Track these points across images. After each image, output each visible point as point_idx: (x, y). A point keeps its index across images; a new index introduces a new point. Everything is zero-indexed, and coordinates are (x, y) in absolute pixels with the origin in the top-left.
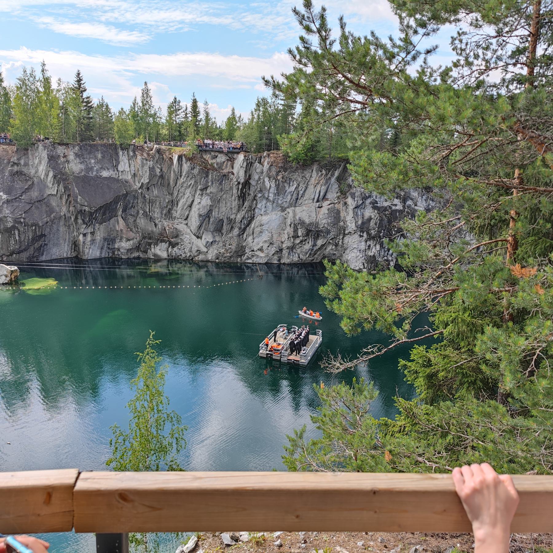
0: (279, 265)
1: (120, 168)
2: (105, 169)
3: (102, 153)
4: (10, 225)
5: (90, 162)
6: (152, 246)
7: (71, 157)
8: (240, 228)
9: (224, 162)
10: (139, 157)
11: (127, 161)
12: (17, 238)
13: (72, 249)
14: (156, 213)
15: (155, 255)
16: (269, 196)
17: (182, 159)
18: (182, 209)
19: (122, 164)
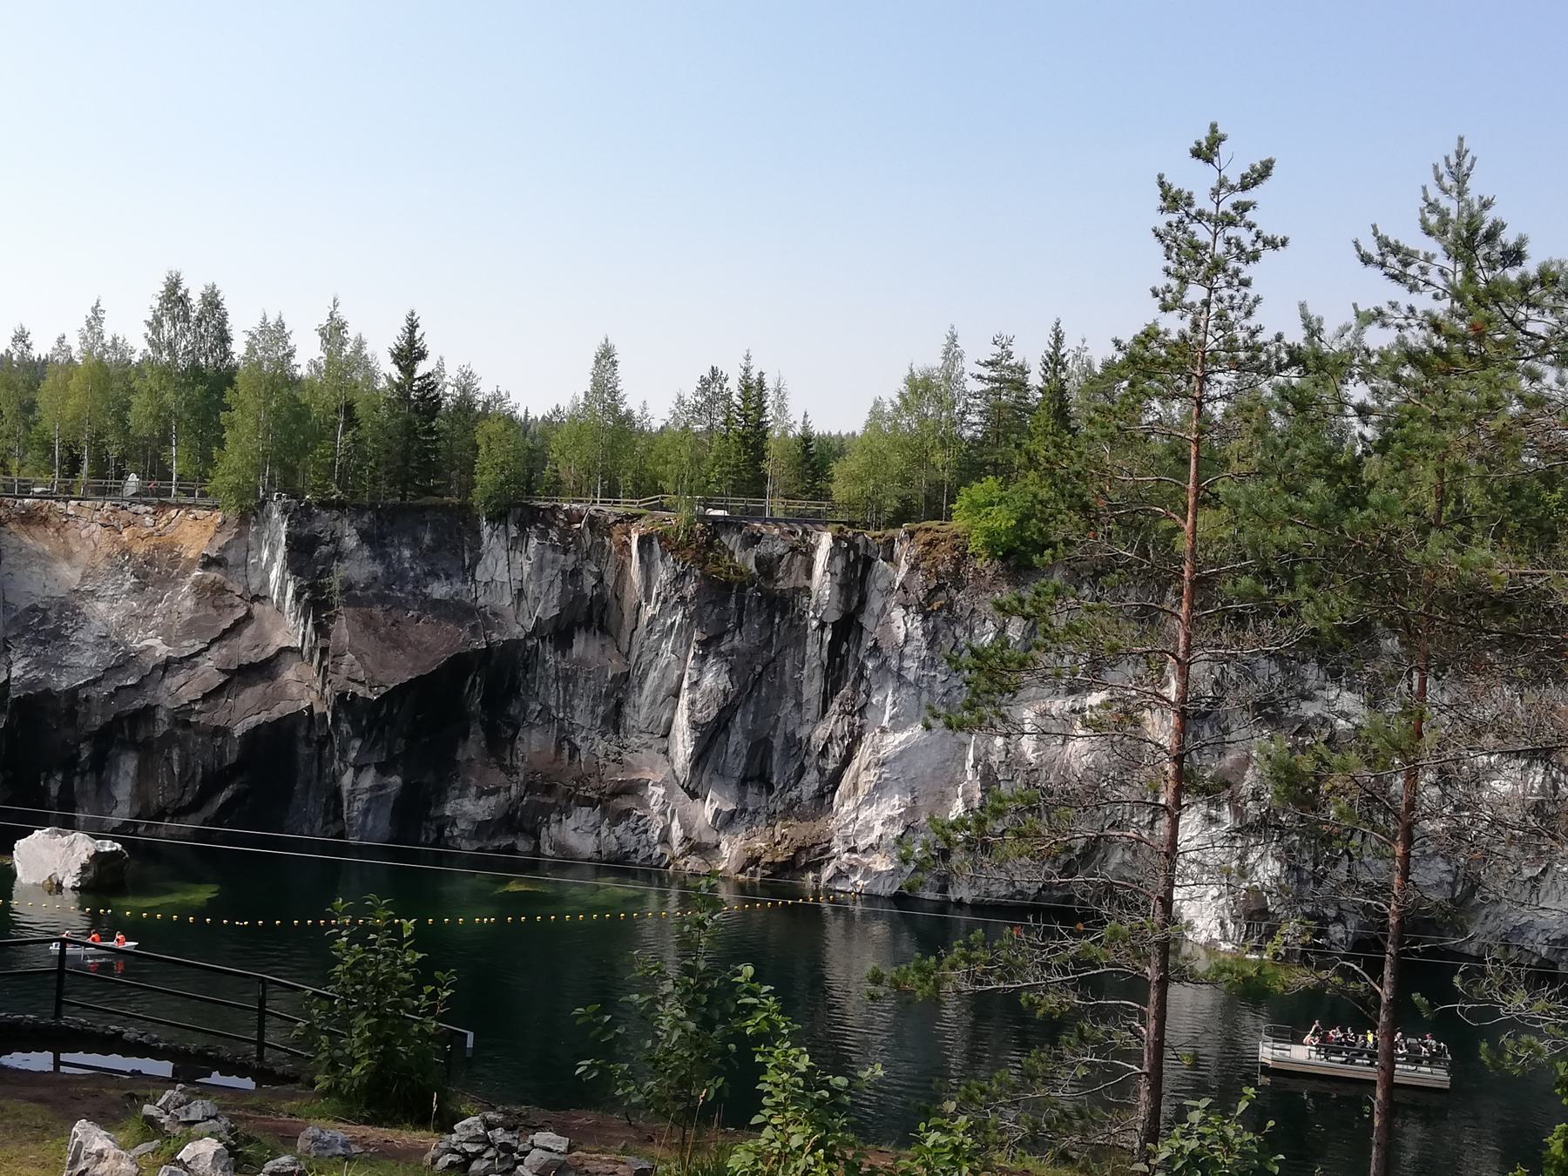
0: (943, 906)
1: (480, 574)
2: (438, 577)
3: (434, 530)
4: (161, 729)
5: (400, 557)
6: (554, 817)
7: (351, 542)
8: (821, 771)
9: (781, 557)
10: (534, 542)
11: (504, 553)
12: (176, 770)
13: (327, 813)
14: (577, 714)
15: (560, 847)
16: (901, 668)
17: (651, 545)
18: (653, 702)
19: (488, 561)
